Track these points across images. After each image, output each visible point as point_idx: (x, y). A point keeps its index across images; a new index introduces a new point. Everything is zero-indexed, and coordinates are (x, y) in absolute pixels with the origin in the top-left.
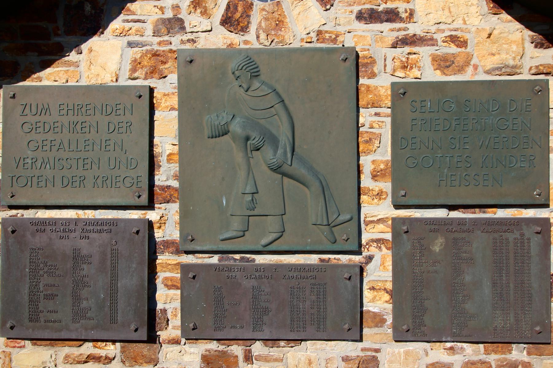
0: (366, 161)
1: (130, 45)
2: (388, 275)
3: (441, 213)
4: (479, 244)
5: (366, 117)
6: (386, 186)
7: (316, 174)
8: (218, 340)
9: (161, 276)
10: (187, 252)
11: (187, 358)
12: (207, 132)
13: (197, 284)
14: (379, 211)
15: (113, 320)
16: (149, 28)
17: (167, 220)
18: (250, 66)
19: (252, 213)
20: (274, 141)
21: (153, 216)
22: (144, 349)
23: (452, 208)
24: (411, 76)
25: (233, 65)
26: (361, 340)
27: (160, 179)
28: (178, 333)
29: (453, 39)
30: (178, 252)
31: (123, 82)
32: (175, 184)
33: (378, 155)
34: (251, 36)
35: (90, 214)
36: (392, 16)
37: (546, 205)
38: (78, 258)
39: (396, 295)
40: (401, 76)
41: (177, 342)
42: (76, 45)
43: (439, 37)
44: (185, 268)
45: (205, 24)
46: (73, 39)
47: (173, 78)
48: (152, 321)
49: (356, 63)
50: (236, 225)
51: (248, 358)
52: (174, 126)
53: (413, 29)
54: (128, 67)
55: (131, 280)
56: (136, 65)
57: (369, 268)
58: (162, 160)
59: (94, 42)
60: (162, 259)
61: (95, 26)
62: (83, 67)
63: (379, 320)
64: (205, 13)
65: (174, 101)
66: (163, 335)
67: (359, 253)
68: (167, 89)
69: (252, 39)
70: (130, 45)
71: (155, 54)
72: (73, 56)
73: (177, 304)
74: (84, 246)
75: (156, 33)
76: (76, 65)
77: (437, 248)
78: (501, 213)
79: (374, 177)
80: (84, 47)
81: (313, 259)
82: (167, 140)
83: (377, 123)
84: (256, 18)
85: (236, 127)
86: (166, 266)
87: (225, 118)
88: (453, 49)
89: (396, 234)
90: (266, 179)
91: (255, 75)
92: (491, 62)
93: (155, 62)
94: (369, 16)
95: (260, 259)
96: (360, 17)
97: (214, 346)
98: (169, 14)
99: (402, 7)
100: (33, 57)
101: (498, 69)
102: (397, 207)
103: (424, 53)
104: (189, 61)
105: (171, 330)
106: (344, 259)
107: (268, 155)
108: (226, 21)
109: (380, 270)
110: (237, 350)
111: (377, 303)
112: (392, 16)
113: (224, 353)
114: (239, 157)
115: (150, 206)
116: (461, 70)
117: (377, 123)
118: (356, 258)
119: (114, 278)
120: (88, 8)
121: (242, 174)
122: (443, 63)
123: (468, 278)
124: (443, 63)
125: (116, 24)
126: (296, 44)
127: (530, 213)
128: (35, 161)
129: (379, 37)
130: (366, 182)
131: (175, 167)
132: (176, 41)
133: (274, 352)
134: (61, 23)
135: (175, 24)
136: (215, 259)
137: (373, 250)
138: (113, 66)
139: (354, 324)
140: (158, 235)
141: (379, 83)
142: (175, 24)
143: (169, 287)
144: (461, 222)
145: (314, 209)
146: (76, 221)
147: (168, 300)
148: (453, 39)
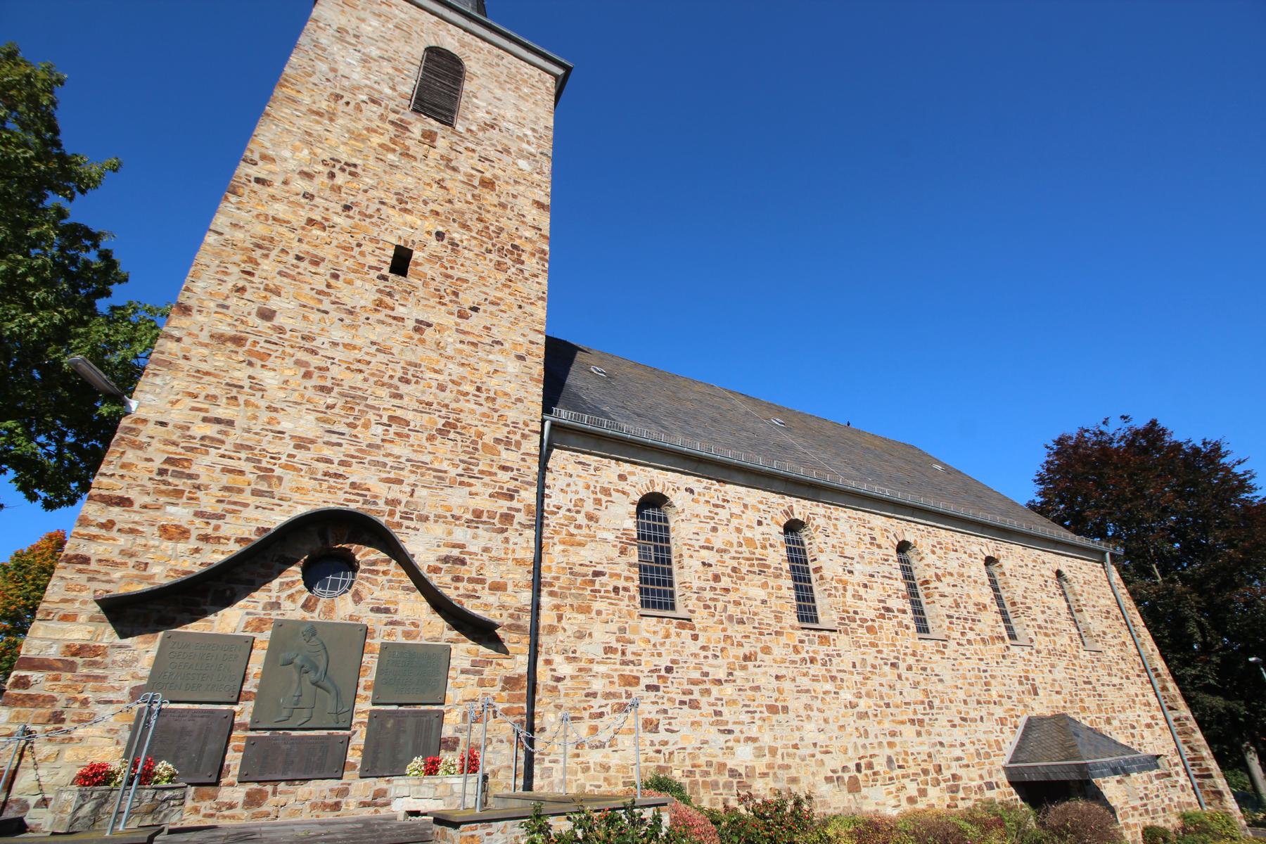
0: (362, 681)
1: (248, 614)
2: (362, 741)
3: (394, 708)
4: (410, 724)
5: (366, 658)
6: (370, 693)
7: (335, 687)
8: (258, 782)
9: (232, 744)
10: (252, 730)
11: (236, 795)
12: (281, 662)
13: (254, 748)
14: (364, 706)
15: (197, 770)
16: (260, 606)
17: (244, 712)
18: (312, 630)
19: (297, 706)
20: (316, 668)
21: (236, 708)
22: (210, 790)
23: (400, 705)
24: (392, 640)
25: (304, 628)
26: (341, 778)
27: (246, 687)
28: (235, 779)
29: (413, 624)
30: (246, 730)
31: (237, 633)
32: (255, 690)
33: (369, 677)
34: (316, 614)
35: (197, 706)
36: (387, 611)
37: (443, 704)
38: (183, 732)
39: (365, 753)
40: (386, 640)
41: (232, 785)
42: (215, 612)
43: (407, 622)
44: (249, 739)
45: (292, 606)
46: (213, 608)
47: (268, 633)
48: (221, 771)
49: (366, 632)
50: (285, 713)
51: (274, 793)
52: (263, 658)
53: (396, 618)
54: (243, 625)
55: (213, 746)
56: (248, 624)
57: (353, 738)
58: (250, 677)
59: (227, 611)
60: (234, 734)
61: (229, 602)
62: (216, 623)
63: (353, 766)
64: (294, 601)
65: (266, 645)
66: (224, 781)
67: (349, 729)
68: (263, 639)
69: (315, 616)
70: (248, 614)
71: (261, 620)
72: (211, 617)
73: (239, 761)
74: (190, 725)
75: (264, 609)
76: (212, 622)
77: (389, 726)
78: (423, 708)
79: (365, 688)
80: (220, 613)
81: (325, 733)
82: (256, 665)
83: (371, 661)
84: (320, 606)
85: (298, 661)
86: (238, 739)
87: (293, 654)
88: (413, 628)
89: (370, 718)
90: (307, 687)
91: (314, 635)
92: (428, 635)
93: (259, 625)
94: (377, 610)
95: (294, 733)
96: (372, 610)
97: (255, 786)
98: (274, 600)
99: (392, 607)
100: (186, 615)
101: (431, 639)
102: (374, 704)
103: (399, 629)
104: (280, 625)
105: (232, 775)
106: (341, 732)
107: (312, 676)
108: (305, 606)
109: (359, 738)
110: (269, 788)
111: (354, 757)
112: (387, 611)
113: (260, 790)
114: (296, 676)
115: (236, 703)
116: (415, 638)
117: (371, 661)
118: (348, 732)
119: (205, 744)
120: (228, 593)
121: (295, 686)
122: (407, 634)
123: (402, 741)
124: (407, 634)
125: (242, 603)
126: (338, 621)
127: (436, 708)
128: (172, 674)
129: (379, 621)
130: (360, 691)
131: (258, 681)
132: (275, 614)
133: (291, 788)
134: (209, 599)
135: (276, 605)
136: (268, 734)
137: (357, 727)
138: (234, 624)
139: (337, 768)
140: (237, 719)
141: (375, 642)
142: (276, 605)
143: (235, 751)
144: (403, 712)
145: (331, 705)
146: (189, 710)
147: (234, 759)
148: (413, 624)
